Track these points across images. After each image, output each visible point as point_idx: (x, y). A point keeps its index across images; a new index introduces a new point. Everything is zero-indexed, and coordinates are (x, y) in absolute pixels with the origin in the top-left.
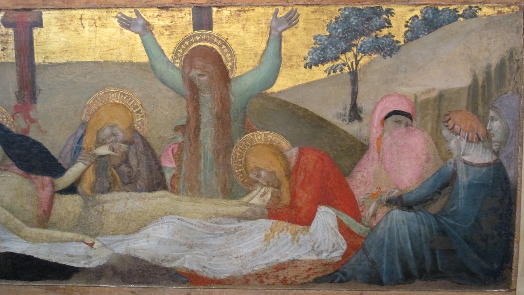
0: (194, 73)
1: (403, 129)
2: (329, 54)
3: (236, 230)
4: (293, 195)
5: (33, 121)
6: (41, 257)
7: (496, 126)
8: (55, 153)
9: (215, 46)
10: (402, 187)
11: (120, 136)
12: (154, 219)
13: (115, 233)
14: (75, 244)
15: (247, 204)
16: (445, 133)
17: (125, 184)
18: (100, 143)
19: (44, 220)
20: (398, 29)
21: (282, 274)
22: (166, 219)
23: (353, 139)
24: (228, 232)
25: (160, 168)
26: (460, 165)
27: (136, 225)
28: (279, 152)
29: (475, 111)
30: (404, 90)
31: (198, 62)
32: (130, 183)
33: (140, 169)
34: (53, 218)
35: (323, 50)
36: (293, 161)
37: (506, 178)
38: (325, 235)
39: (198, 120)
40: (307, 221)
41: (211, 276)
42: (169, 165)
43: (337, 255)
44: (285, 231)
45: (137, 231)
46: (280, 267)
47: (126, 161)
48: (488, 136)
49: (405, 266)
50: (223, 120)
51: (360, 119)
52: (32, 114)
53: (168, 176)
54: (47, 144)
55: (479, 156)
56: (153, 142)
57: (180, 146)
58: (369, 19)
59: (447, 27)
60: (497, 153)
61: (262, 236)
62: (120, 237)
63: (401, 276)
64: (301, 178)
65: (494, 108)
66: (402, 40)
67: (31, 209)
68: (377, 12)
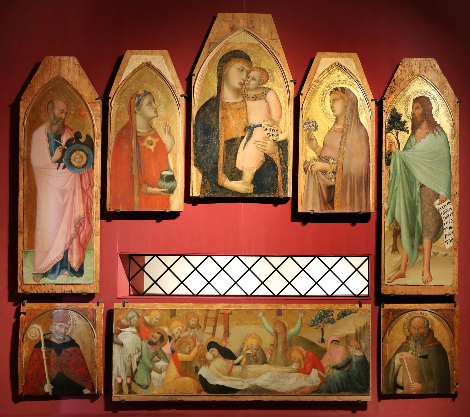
0: (276, 329)
1: (336, 345)
2: (316, 323)
3: (288, 376)
4: (305, 365)
5: (228, 343)
6: (227, 386)
7: (363, 345)
8: (234, 352)
9: (283, 321)
10: (337, 363)
11: (254, 347)
12: (263, 373)
13: (251, 378)
14: (239, 382)
15: (291, 368)
16: (349, 346)
17: (255, 362)
18: (248, 350)
19: (229, 374)
20: (335, 317)
21: (301, 390)
22: (267, 373)
23: (322, 348)
24: (285, 377)
25: (266, 357)
26: (353, 356)
27: (257, 375)
28: (301, 353)
29: (357, 340)
30: (336, 334)
31: (278, 325)
32: (256, 362)
33: (260, 358)
34: (232, 373)
35: (314, 322)
36: (305, 355)
37: (366, 360)
38: (314, 378)
39: (277, 343)
40: (309, 373)
41: (280, 391)
42: (268, 356)
43: (318, 384)
44: (303, 376)
45: (258, 377)
46: (301, 388)
47: (256, 355)
48: (361, 348)
49: (338, 387)
50: (285, 342)
51: (324, 342)
52: (228, 341)
53: (268, 360)
54: (232, 350)
55: (359, 353)
56: (264, 349)
57: (272, 351)
58: (327, 313)
59: (348, 316)
60: (364, 353)
61: (296, 378)
62: (252, 379)
63: (337, 391)
64: (307, 360)
65: (362, 339)
66: (336, 319)
67: (225, 370)
68: (329, 311)
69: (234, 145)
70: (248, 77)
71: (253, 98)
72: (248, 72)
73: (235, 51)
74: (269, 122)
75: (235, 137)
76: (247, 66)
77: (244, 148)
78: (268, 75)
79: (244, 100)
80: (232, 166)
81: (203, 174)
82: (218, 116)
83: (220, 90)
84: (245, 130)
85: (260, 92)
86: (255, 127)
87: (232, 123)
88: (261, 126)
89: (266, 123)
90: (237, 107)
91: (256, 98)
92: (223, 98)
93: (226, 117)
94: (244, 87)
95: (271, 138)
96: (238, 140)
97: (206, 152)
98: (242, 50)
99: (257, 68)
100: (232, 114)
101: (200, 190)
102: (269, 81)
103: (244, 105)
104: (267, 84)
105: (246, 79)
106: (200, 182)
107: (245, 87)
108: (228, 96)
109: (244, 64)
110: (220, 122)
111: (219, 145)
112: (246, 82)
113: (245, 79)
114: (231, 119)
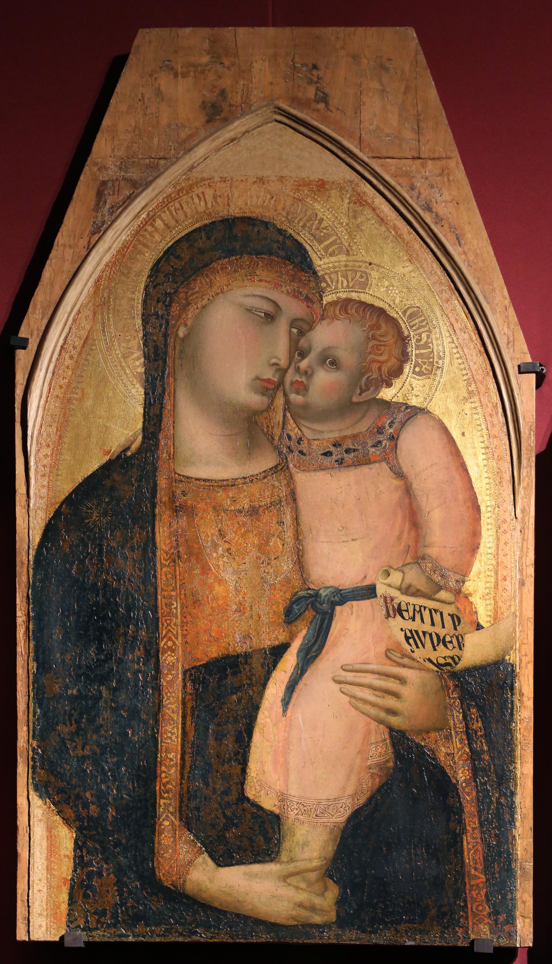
69: (237, 689)
70: (298, 351)
71: (328, 454)
72: (301, 328)
73: (229, 223)
74: (413, 576)
75: (236, 644)
76: (296, 294)
77: (286, 702)
78: (403, 340)
79: (282, 468)
80: (226, 793)
81: (80, 830)
82: (150, 542)
83: (160, 418)
84: (288, 612)
85: (364, 426)
86: (342, 597)
87: (221, 581)
88: (370, 592)
89: (396, 578)
90: (245, 504)
91: (346, 455)
92: (172, 457)
93: (190, 552)
94: (280, 401)
95: (419, 654)
96: (256, 663)
97: (91, 721)
98: (268, 215)
99: (345, 305)
100: (222, 534)
101: (64, 907)
102: (407, 368)
103: (284, 492)
104: (397, 383)
105: (291, 359)
106: (66, 868)
107: (287, 402)
108: (202, 448)
109: (277, 286)
110: (163, 573)
111: (158, 689)
112: (291, 376)
113: (283, 363)
114: (217, 558)
